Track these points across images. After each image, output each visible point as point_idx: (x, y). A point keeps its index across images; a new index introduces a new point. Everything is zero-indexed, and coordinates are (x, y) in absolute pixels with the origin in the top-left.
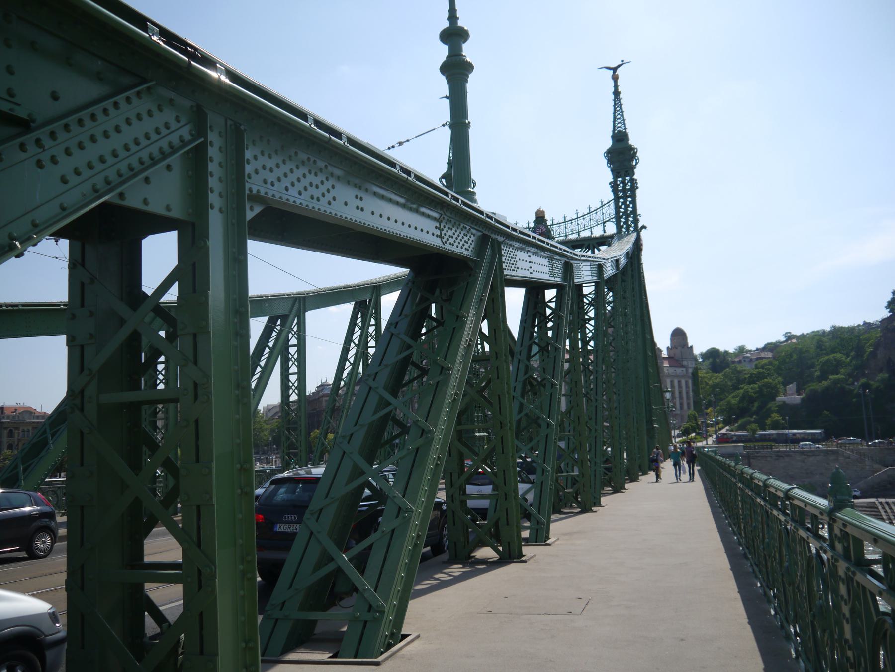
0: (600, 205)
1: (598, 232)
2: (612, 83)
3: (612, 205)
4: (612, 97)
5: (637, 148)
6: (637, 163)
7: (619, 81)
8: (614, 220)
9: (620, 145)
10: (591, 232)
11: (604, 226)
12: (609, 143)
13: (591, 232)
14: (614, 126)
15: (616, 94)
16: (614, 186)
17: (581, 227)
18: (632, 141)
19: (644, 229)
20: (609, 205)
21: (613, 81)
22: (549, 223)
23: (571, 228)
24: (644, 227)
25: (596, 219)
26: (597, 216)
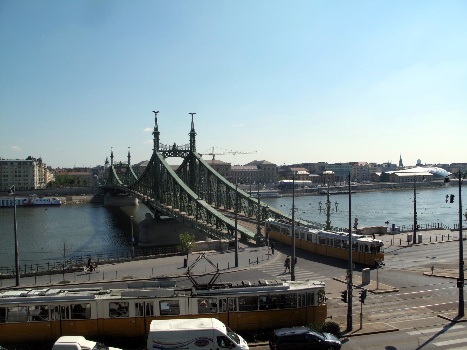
1: (187, 149)
18: (196, 131)
22: (177, 146)
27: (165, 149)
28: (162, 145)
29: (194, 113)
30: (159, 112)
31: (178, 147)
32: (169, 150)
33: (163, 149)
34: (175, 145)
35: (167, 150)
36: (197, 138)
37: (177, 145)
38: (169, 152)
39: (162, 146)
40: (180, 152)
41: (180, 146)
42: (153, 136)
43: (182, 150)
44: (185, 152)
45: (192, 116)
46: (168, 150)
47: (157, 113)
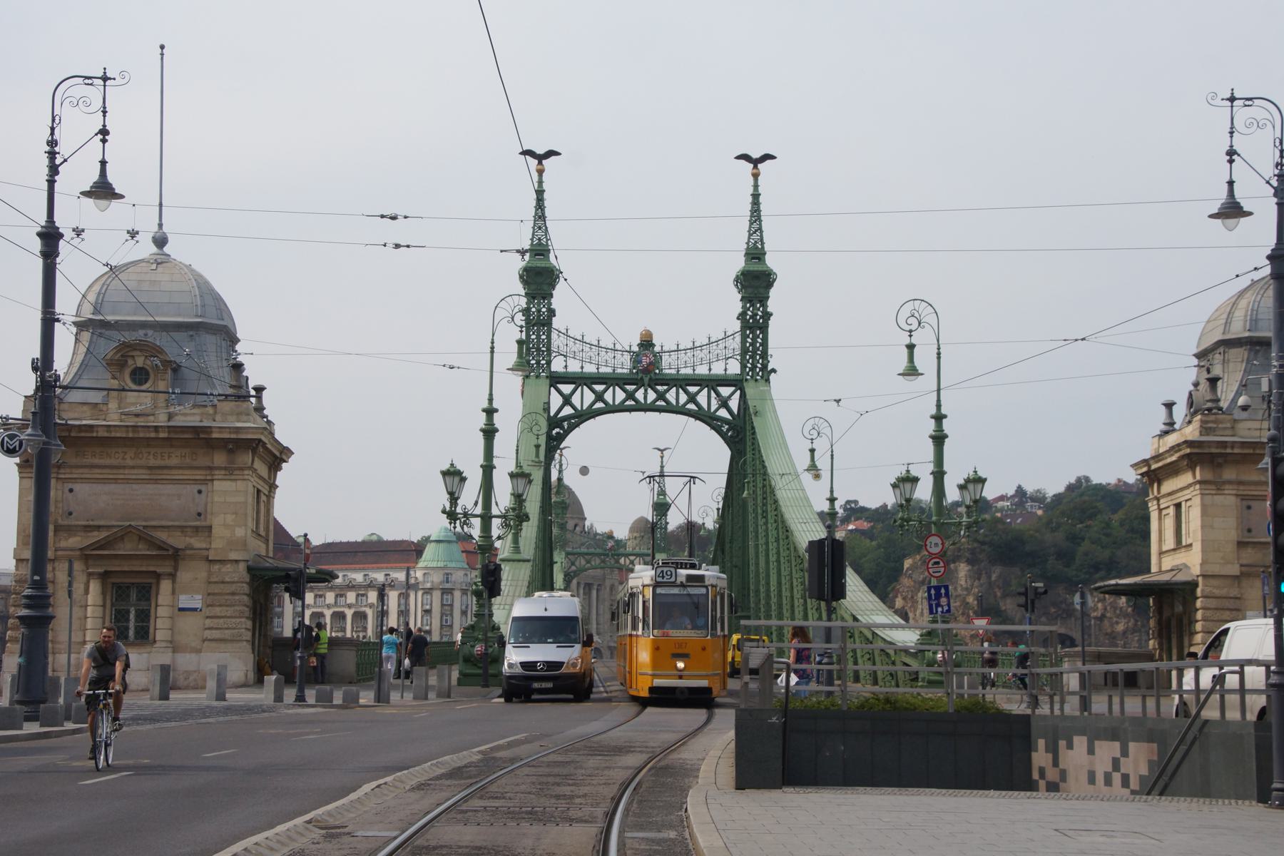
0: (723, 336)
1: (718, 369)
2: (751, 180)
3: (738, 338)
4: (750, 199)
5: (775, 274)
7: (759, 178)
8: (739, 357)
9: (756, 267)
10: (710, 370)
11: (726, 364)
13: (710, 370)
14: (750, 235)
15: (756, 196)
16: (742, 317)
17: (697, 361)
18: (771, 261)
20: (733, 339)
22: (657, 349)
23: (684, 360)
24: (774, 371)
25: (716, 353)
27: (590, 369)
28: (571, 342)
30: (557, 154)
32: (609, 370)
33: (574, 367)
34: (647, 343)
35: (598, 369)
36: (776, 300)
40: (681, 382)
43: (689, 371)
44: (712, 383)
46: (603, 370)
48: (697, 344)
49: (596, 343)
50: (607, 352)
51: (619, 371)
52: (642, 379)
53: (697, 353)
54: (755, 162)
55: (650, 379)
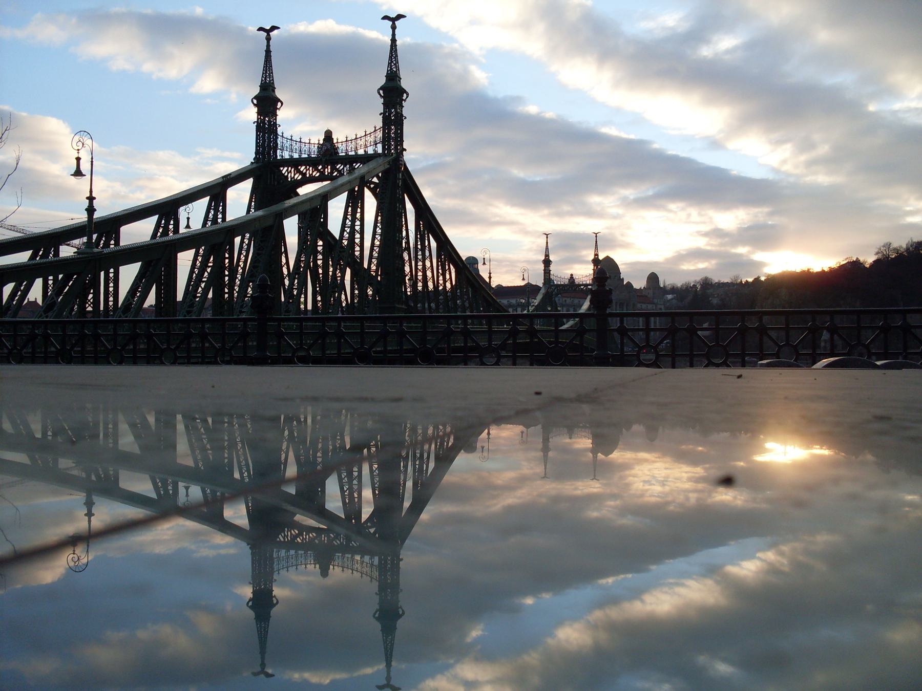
1: (370, 151)
6: (407, 97)
7: (396, 30)
12: (382, 81)
19: (404, 152)
20: (380, 131)
21: (391, 30)
22: (335, 141)
26: (371, 139)
27: (296, 156)
29: (400, 17)
31: (340, 145)
32: (306, 156)
33: (286, 155)
34: (328, 136)
37: (338, 137)
38: (310, 162)
39: (288, 144)
41: (347, 141)
42: (256, 109)
43: (353, 153)
45: (394, 28)
46: (304, 156)
47: (270, 33)
48: (358, 136)
49: (299, 140)
50: (305, 145)
51: (313, 156)
52: (321, 160)
53: (359, 141)
54: (394, 20)
55: (326, 160)
